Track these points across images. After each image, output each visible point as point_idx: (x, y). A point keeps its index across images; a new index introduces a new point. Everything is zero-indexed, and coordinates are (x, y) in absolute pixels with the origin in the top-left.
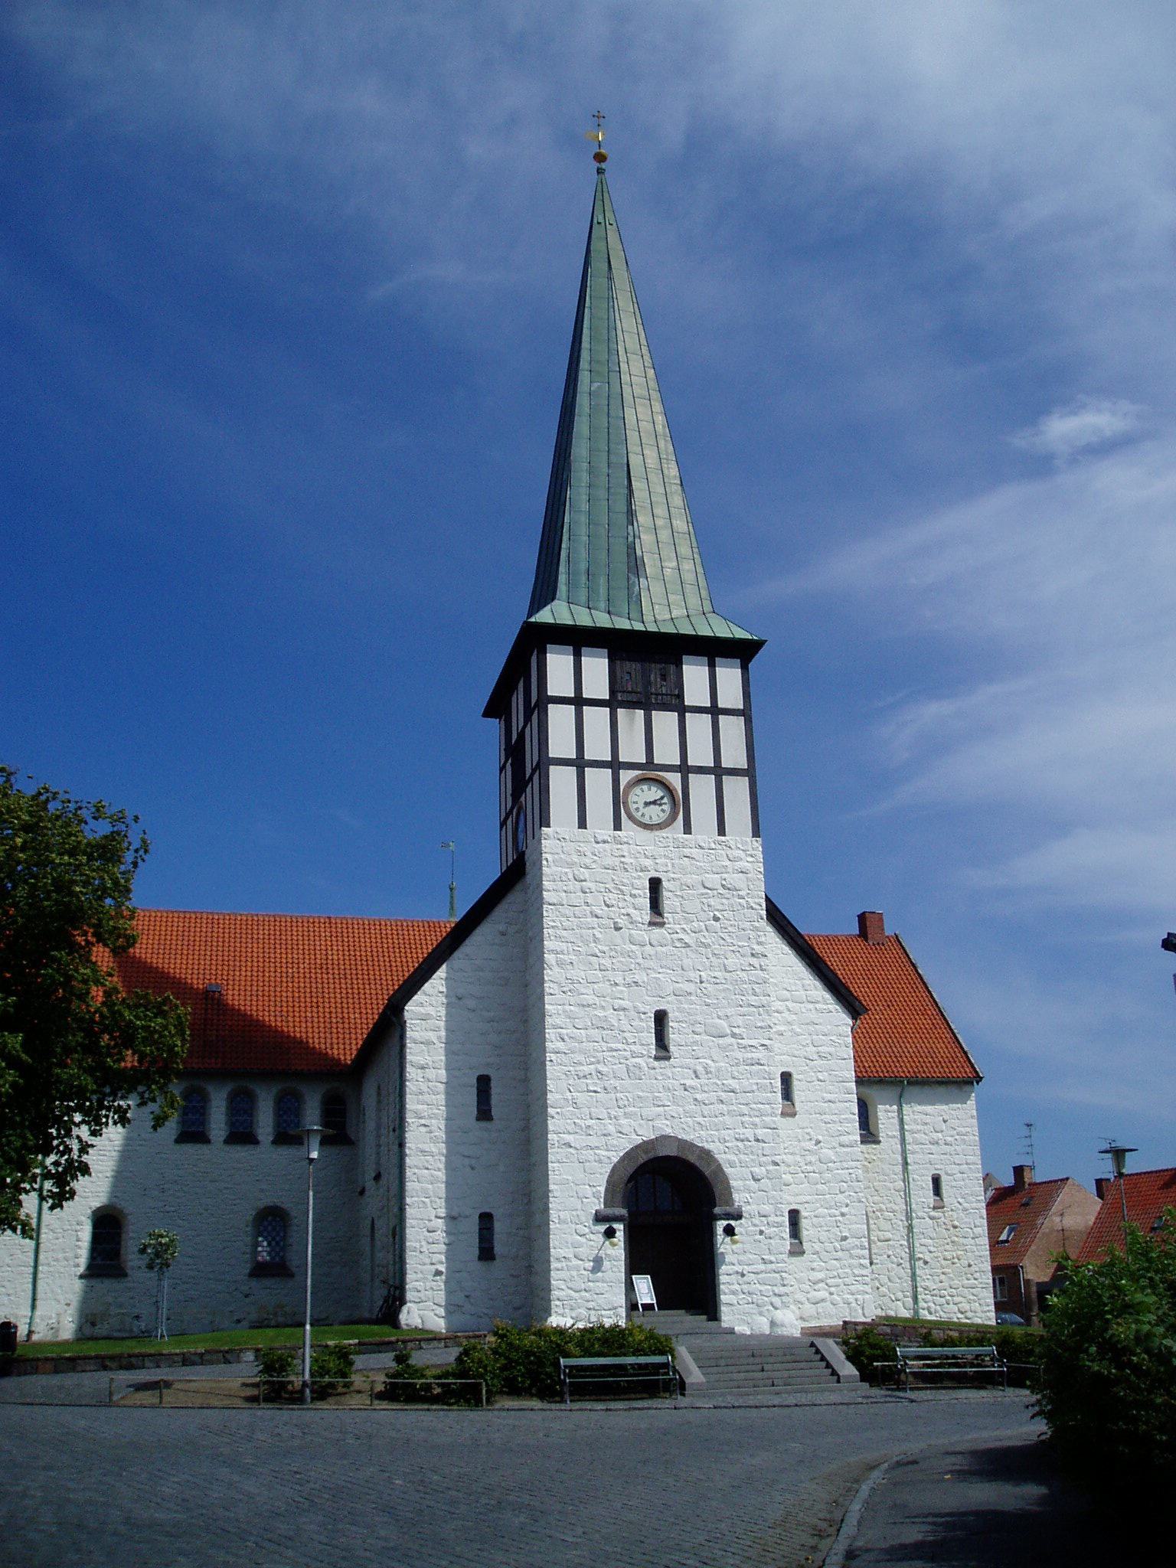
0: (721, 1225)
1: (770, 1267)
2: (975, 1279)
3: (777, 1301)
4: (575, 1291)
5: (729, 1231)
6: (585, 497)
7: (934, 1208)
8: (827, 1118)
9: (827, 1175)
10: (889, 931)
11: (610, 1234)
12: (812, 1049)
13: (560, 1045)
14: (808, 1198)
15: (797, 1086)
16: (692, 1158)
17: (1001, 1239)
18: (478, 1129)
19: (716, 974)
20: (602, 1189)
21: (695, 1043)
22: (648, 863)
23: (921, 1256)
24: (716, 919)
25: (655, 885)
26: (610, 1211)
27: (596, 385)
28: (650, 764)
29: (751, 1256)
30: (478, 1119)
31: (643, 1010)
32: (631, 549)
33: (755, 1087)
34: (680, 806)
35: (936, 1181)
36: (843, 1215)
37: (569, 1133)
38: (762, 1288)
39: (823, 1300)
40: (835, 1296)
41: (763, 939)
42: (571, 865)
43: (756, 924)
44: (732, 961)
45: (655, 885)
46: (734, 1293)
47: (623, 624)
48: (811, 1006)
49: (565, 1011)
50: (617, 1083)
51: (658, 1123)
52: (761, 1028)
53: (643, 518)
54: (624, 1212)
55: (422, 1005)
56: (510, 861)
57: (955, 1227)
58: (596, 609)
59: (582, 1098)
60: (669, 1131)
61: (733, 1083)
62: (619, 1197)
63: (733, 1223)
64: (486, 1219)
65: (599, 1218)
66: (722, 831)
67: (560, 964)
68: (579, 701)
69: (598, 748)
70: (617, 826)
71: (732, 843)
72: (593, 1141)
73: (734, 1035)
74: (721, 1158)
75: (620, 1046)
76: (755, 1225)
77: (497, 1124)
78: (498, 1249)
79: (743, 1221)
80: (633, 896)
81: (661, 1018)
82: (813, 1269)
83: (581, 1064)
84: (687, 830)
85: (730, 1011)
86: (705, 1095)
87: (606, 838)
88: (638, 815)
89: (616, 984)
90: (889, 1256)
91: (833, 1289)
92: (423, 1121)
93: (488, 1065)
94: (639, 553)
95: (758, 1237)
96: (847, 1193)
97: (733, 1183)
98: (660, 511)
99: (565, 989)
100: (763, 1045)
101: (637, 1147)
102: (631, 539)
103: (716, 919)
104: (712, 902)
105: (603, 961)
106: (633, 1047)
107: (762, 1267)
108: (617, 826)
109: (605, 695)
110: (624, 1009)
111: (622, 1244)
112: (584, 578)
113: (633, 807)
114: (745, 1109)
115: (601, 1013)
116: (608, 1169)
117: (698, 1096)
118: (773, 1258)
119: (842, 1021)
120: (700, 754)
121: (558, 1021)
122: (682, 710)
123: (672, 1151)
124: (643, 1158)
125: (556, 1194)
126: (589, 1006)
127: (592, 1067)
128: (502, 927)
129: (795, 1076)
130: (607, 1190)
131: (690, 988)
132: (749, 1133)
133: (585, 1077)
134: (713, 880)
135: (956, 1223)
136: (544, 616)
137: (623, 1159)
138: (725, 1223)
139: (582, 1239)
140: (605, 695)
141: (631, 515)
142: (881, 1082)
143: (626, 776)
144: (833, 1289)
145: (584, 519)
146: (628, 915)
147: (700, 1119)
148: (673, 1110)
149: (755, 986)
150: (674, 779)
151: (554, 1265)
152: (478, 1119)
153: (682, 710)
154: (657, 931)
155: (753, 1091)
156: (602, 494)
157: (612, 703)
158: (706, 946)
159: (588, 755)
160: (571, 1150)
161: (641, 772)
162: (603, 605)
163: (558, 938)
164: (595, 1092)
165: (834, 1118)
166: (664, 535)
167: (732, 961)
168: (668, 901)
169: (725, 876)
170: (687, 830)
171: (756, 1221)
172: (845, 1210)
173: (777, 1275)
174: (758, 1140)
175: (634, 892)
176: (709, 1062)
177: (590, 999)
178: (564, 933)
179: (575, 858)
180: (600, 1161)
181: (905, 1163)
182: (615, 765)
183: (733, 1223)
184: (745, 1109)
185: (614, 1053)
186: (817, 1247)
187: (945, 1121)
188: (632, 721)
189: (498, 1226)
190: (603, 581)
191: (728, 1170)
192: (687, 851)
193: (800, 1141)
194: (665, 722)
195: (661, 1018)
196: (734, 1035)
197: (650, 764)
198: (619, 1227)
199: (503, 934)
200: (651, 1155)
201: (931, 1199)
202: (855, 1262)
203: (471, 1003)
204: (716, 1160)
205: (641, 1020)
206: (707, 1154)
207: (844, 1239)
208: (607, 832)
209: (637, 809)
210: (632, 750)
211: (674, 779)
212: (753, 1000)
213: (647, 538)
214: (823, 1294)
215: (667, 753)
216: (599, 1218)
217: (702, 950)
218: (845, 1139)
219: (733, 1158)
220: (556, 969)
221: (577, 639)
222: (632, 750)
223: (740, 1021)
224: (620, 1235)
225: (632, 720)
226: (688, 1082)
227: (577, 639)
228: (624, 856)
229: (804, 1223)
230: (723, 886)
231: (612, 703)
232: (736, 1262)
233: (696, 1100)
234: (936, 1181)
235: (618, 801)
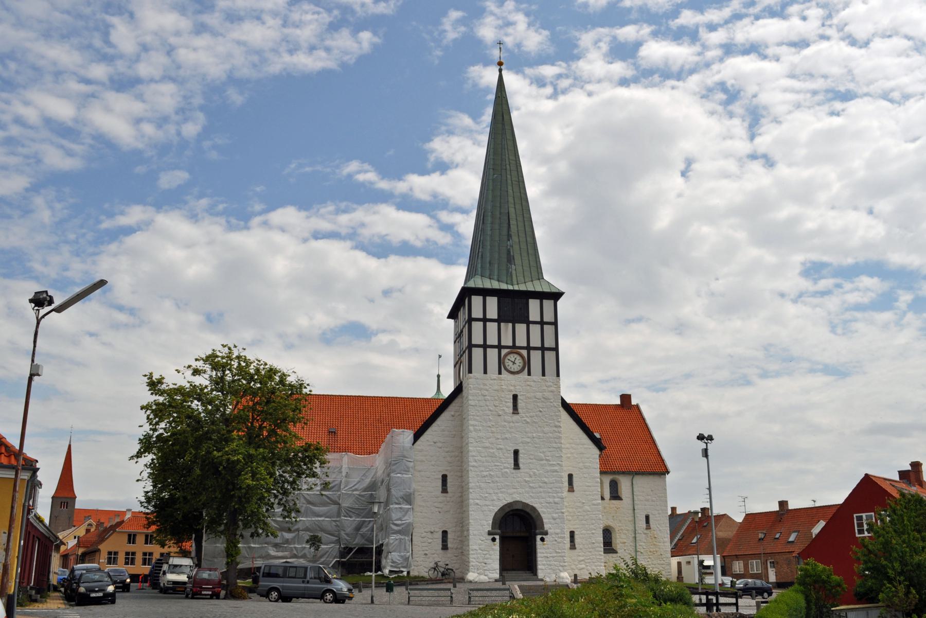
0: (538, 537)
1: (558, 555)
2: (664, 561)
3: (560, 568)
4: (479, 563)
5: (542, 540)
6: (489, 228)
7: (646, 529)
8: (587, 493)
9: (586, 517)
10: (634, 402)
11: (494, 540)
12: (582, 464)
13: (474, 464)
14: (578, 526)
15: (575, 479)
16: (528, 510)
17: (693, 542)
18: (442, 497)
19: (540, 434)
20: (491, 522)
21: (531, 463)
22: (512, 388)
23: (639, 550)
24: (541, 411)
25: (515, 397)
26: (494, 531)
27: (496, 175)
28: (514, 346)
29: (551, 550)
30: (442, 492)
31: (509, 449)
32: (509, 252)
33: (554, 481)
34: (527, 364)
35: (647, 518)
36: (593, 533)
37: (478, 499)
38: (556, 563)
39: (583, 568)
40: (588, 567)
41: (560, 420)
42: (481, 389)
43: (557, 414)
44: (546, 429)
45: (515, 397)
46: (544, 565)
47: (504, 286)
48: (581, 446)
49: (477, 450)
50: (497, 479)
51: (514, 496)
52: (558, 457)
53: (515, 238)
54: (499, 531)
55: (419, 445)
56: (457, 385)
57: (655, 538)
58: (493, 279)
59: (483, 485)
60: (518, 499)
61: (546, 480)
62: (497, 526)
63: (544, 536)
64: (445, 533)
65: (490, 533)
66: (544, 375)
67: (475, 430)
68: (485, 320)
69: (492, 340)
70: (500, 373)
71: (548, 379)
72: (488, 503)
73: (547, 460)
74: (540, 510)
75: (499, 464)
76: (553, 538)
77: (450, 494)
78: (449, 545)
79: (548, 536)
80: (506, 402)
81: (516, 453)
82: (580, 556)
83: (482, 471)
84: (529, 374)
85: (545, 450)
86: (534, 485)
87: (495, 378)
88: (509, 368)
89: (498, 439)
90: (625, 550)
91: (588, 564)
92: (419, 493)
93: (447, 470)
94: (512, 254)
95: (554, 542)
96: (595, 525)
97: (545, 521)
98: (522, 235)
99: (477, 441)
100: (558, 464)
101: (505, 505)
102: (509, 247)
103: (541, 411)
104: (538, 404)
105: (493, 429)
106: (505, 465)
107: (555, 555)
108: (500, 373)
109: (496, 317)
110: (501, 449)
111: (498, 544)
112: (488, 265)
113: (507, 364)
114: (550, 490)
115: (492, 451)
116: (494, 514)
117: (531, 485)
118: (560, 551)
119: (596, 452)
120: (535, 342)
121: (474, 454)
122: (528, 323)
123: (520, 507)
124: (508, 510)
125: (472, 524)
126: (487, 447)
127: (487, 473)
128: (452, 413)
129: (574, 476)
130: (493, 522)
131: (528, 440)
132: (551, 500)
133: (484, 477)
134: (539, 395)
135: (656, 536)
136: (471, 284)
137: (499, 510)
138: (541, 536)
139: (483, 542)
140: (496, 317)
141: (509, 236)
142: (623, 473)
143: (504, 352)
144: (588, 564)
145: (488, 238)
146: (504, 410)
147: (531, 494)
148: (520, 490)
149: (556, 440)
150: (524, 352)
151: (471, 552)
152: (442, 492)
153: (528, 323)
154: (516, 417)
155: (554, 483)
156: (497, 227)
157: (499, 321)
158: (535, 422)
159: (488, 343)
160: (479, 506)
162: (496, 277)
163: (475, 420)
164: (489, 483)
165: (591, 493)
166: (523, 246)
167: (546, 429)
168: (521, 404)
169: (545, 393)
170: (529, 374)
171: (553, 536)
172: (594, 531)
173: (561, 558)
174: (555, 503)
175: (506, 400)
176: (535, 471)
177: (487, 445)
178: (477, 418)
179: (482, 387)
180: (490, 511)
181: (634, 509)
182: (499, 347)
183: (544, 536)
184: (550, 490)
185: (496, 467)
186: (581, 546)
187: (652, 491)
188: (507, 328)
189: (449, 536)
190: (496, 266)
191: (543, 515)
192: (528, 383)
193: (575, 502)
194: (521, 328)
195: (516, 453)
196: (547, 460)
197: (514, 346)
198: (497, 537)
199: (453, 416)
200: (511, 508)
201: (644, 525)
202: (597, 553)
203: (440, 445)
204: (538, 511)
205: (509, 453)
206: (534, 509)
207: (594, 543)
208: (496, 375)
209: (508, 365)
210: (507, 341)
211: (524, 352)
212: (554, 445)
213: (516, 247)
214: (583, 566)
215: (521, 341)
216: (490, 533)
217: (534, 424)
218: (594, 502)
219: (545, 510)
220: (474, 433)
221: (485, 293)
222: (507, 341)
223: (549, 454)
224: (498, 541)
225: (507, 329)
226: (527, 479)
227: (485, 293)
228: (502, 385)
229: (576, 537)
230: (544, 398)
231: (499, 321)
232: (544, 552)
233: (530, 486)
234: (647, 518)
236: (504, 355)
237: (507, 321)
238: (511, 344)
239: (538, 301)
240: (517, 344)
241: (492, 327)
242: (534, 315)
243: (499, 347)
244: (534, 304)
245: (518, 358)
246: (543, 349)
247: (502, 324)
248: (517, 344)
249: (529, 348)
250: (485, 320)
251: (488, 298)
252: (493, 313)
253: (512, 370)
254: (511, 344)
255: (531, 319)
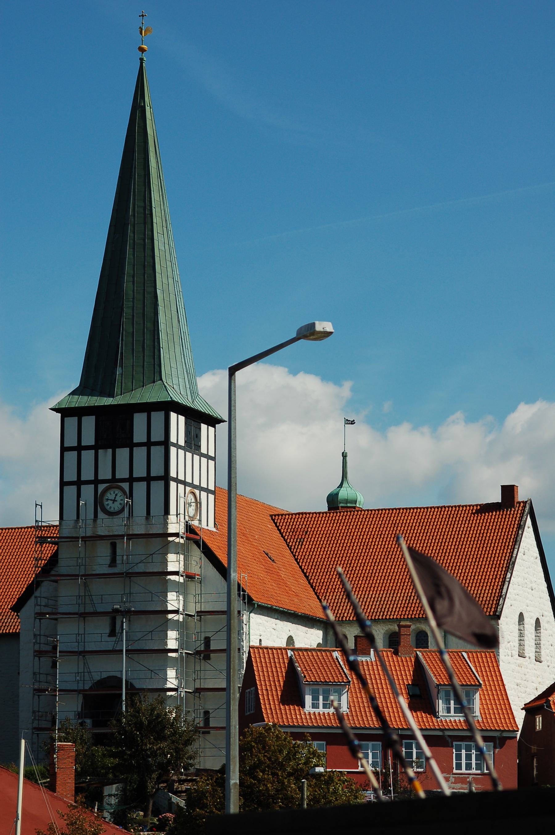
109: (92, 442)
120: (140, 471)
122: (131, 445)
140: (92, 442)
143: (101, 487)
150: (126, 486)
153: (131, 445)
157: (95, 448)
161: (108, 484)
188: (106, 456)
194: (123, 453)
210: (105, 473)
215: (122, 472)
222: (105, 473)
231: (95, 448)
235: (98, 501)
236: (102, 492)
237: (105, 447)
238: (110, 477)
239: (144, 415)
240: (118, 476)
241: (88, 456)
242: (139, 435)
243: (96, 482)
244: (139, 420)
245: (120, 493)
246: (149, 479)
247: (100, 451)
248: (118, 476)
249: (131, 480)
250: (79, 448)
251: (85, 419)
252: (89, 438)
253: (112, 510)
254: (110, 477)
255: (135, 440)
